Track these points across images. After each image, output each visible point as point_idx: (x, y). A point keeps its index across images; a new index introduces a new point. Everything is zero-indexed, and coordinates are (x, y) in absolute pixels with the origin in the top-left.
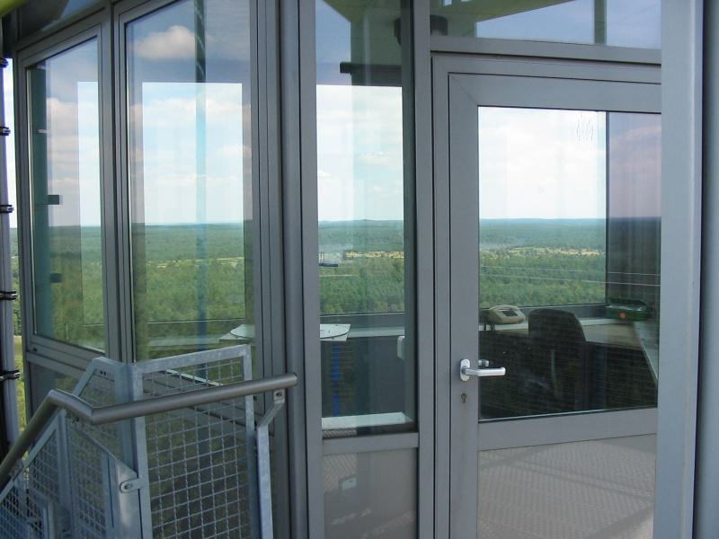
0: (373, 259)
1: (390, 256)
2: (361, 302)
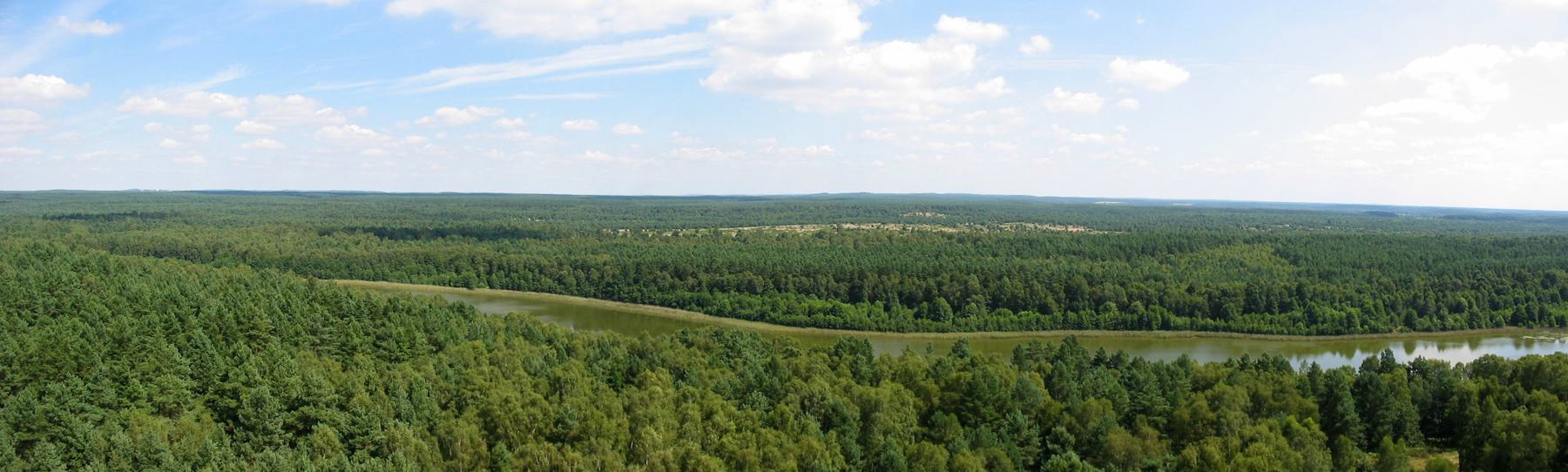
0: (869, 232)
1: (886, 227)
2: (852, 273)
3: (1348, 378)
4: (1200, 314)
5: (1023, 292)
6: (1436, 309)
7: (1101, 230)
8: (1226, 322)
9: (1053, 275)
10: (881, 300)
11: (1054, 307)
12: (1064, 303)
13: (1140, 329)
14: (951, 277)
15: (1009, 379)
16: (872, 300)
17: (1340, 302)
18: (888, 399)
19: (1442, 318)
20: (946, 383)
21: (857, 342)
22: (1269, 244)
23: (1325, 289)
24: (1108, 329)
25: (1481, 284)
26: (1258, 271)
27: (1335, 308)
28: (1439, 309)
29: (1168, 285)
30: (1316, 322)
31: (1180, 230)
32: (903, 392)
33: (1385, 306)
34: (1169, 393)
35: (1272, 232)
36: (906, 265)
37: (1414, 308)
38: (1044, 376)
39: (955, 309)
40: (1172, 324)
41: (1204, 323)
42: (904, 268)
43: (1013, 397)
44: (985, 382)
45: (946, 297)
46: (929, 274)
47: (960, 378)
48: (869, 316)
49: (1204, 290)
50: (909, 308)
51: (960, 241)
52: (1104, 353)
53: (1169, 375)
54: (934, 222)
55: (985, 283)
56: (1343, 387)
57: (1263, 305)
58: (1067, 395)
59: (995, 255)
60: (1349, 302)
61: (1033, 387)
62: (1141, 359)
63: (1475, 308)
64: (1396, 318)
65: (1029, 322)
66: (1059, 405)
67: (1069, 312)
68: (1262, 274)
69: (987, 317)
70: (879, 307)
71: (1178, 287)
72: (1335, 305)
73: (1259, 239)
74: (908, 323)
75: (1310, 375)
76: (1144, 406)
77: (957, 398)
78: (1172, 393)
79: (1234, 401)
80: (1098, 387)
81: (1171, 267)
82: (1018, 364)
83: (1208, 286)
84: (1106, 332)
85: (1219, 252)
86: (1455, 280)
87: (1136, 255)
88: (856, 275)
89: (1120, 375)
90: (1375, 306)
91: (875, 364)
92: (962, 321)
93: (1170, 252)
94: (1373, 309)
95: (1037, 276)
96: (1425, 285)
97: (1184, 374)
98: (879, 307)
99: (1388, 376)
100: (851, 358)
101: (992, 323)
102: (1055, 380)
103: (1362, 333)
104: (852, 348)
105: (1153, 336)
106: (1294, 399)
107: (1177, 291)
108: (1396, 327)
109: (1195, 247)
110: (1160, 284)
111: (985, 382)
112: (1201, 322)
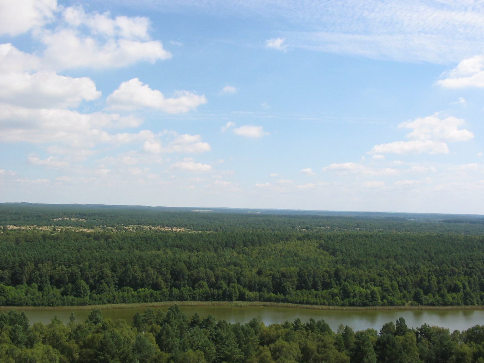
0: (27, 231)
1: (40, 229)
2: (14, 263)
3: (373, 339)
4: (265, 290)
5: (141, 275)
6: (437, 289)
7: (197, 230)
8: (285, 296)
9: (162, 262)
10: (37, 283)
11: (163, 284)
12: (170, 282)
13: (224, 300)
14: (89, 264)
15: (130, 338)
16: (29, 283)
17: (366, 282)
18: (41, 357)
19: (442, 296)
20: (84, 342)
21: (15, 315)
22: (316, 241)
23: (355, 273)
24: (201, 300)
25: (473, 272)
26: (307, 260)
27: (362, 287)
28: (440, 289)
29: (243, 269)
30: (348, 297)
31: (253, 231)
32: (51, 351)
33: (400, 286)
34: (243, 346)
35: (317, 232)
36: (55, 256)
37: (420, 288)
38: (155, 334)
39: (92, 288)
40: (246, 297)
41: (268, 296)
42: (54, 258)
43: (133, 350)
44: (113, 341)
45: (87, 280)
46: (73, 263)
47: (94, 338)
48: (26, 294)
49: (269, 272)
50: (57, 288)
51: (97, 238)
52: (198, 317)
53: (244, 333)
54: (77, 224)
55: (114, 270)
56: (368, 344)
57: (310, 284)
58: (172, 348)
59: (121, 249)
60: (373, 283)
61: (148, 343)
62: (224, 321)
63: (468, 288)
64: (408, 295)
65: (146, 296)
66: (167, 356)
67: (174, 288)
68: (310, 262)
69: (115, 293)
70: (35, 288)
71: (251, 270)
72: (362, 284)
73: (308, 237)
74: (57, 299)
75: (343, 335)
76: (226, 355)
77: (93, 353)
78: (246, 346)
79: (289, 353)
80: (194, 342)
81: (246, 256)
82: (136, 327)
83: (271, 270)
84: (200, 303)
85: (280, 246)
86: (452, 268)
87: (222, 248)
88: (17, 264)
89: (209, 333)
90: (392, 286)
91: (30, 331)
92: (97, 296)
93: (245, 246)
94: (390, 288)
95: (151, 263)
96: (429, 271)
97: (254, 332)
98: (35, 288)
99: (402, 338)
100: (10, 328)
101: (118, 297)
102: (163, 337)
103: (382, 305)
104: (12, 320)
105: (233, 305)
106: (333, 353)
107: (250, 274)
108: (407, 301)
109: (262, 242)
110: (238, 268)
111: (113, 341)
112: (267, 295)
